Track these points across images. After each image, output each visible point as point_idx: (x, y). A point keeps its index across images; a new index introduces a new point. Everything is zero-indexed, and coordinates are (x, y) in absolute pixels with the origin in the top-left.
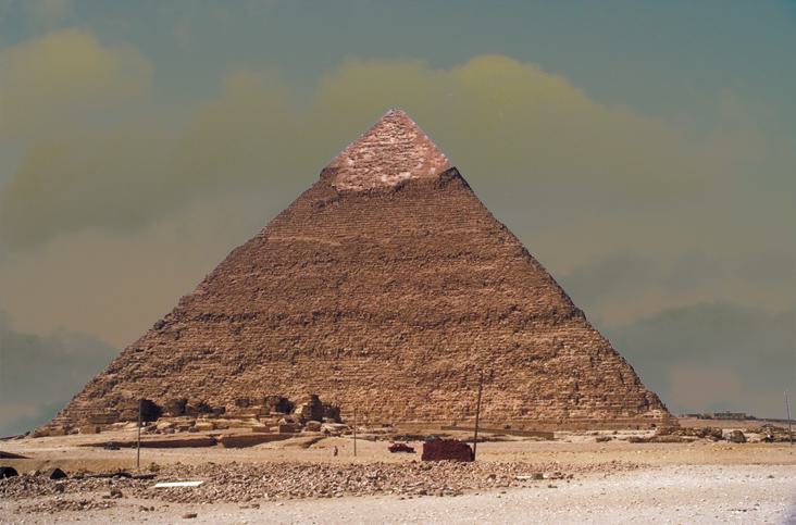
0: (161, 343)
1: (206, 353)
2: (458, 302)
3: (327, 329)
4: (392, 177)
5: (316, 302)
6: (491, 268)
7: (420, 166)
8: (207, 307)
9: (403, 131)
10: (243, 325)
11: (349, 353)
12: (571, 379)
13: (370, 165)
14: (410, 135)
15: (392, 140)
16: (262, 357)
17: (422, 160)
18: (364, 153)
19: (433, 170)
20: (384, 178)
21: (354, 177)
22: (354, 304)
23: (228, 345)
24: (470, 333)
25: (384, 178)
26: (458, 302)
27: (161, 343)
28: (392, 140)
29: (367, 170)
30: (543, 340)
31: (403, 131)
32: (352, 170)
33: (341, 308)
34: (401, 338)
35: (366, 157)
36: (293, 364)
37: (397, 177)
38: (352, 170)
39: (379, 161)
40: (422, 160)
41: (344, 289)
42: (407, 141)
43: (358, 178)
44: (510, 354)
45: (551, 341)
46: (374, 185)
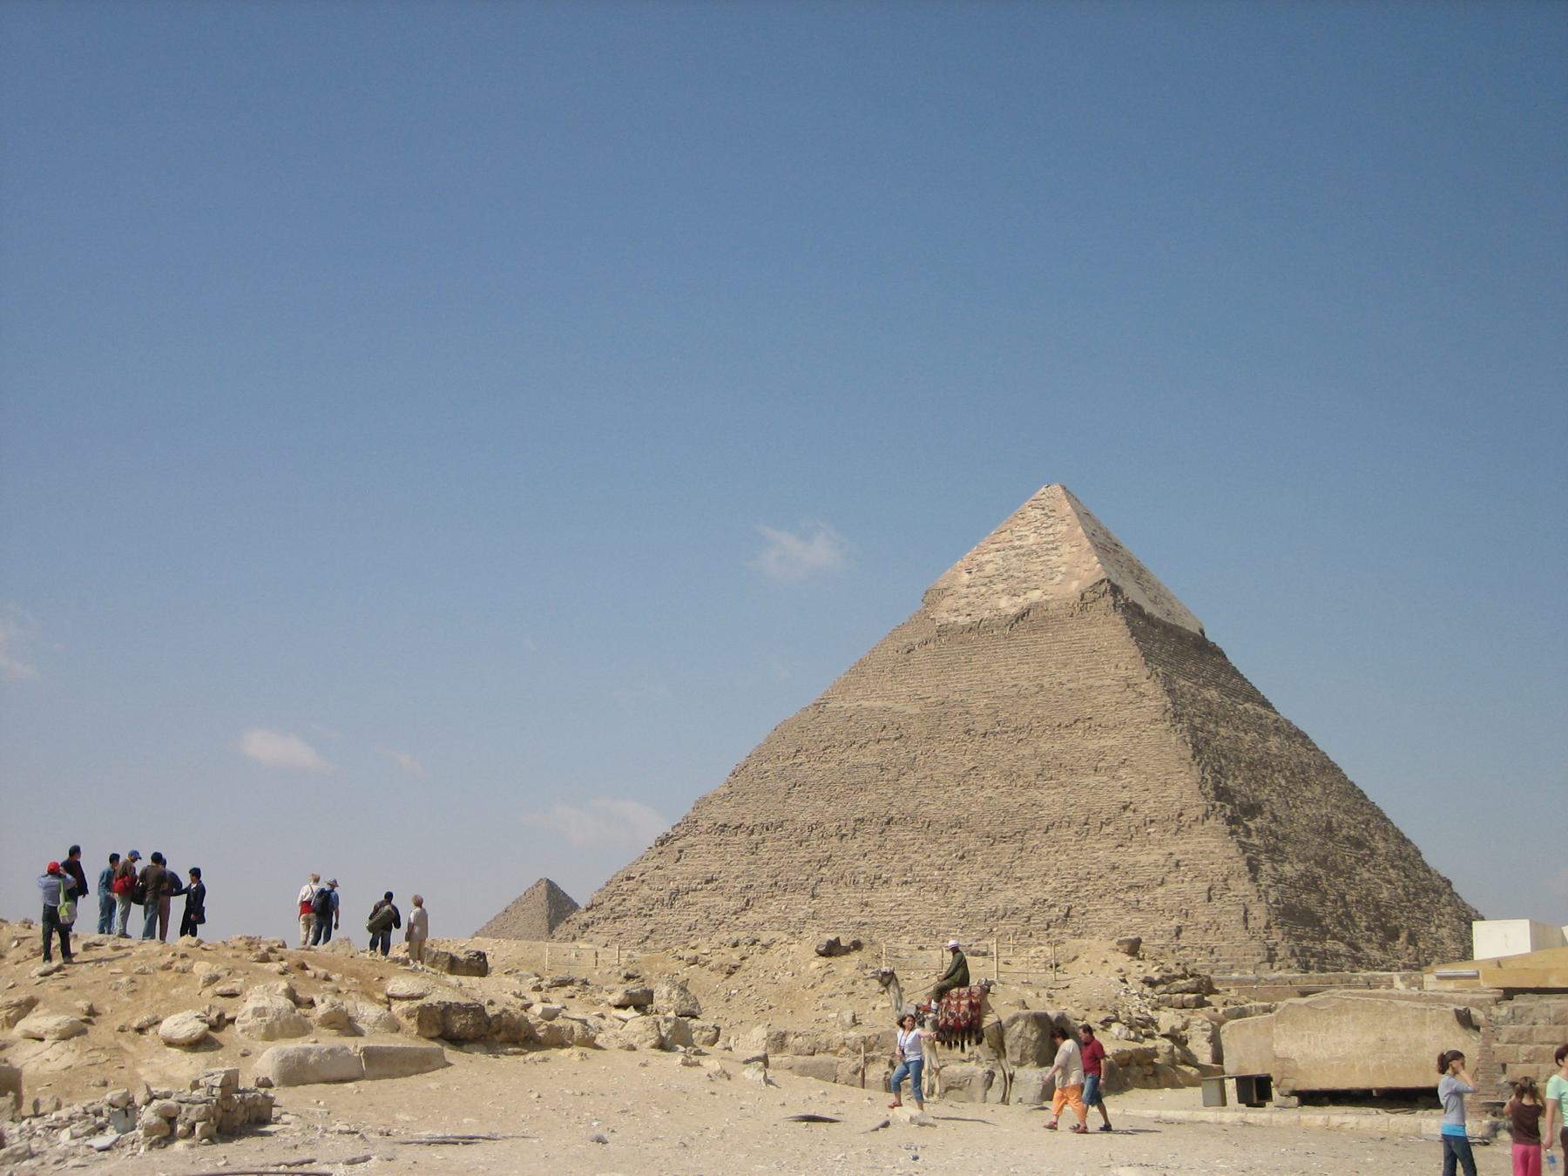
1: (707, 882)
2: (1051, 800)
3: (870, 845)
5: (866, 802)
7: (1059, 578)
8: (721, 814)
9: (1050, 521)
10: (764, 841)
13: (990, 580)
14: (1059, 528)
15: (1032, 539)
16: (778, 886)
19: (1075, 584)
21: (964, 601)
22: (911, 805)
23: (735, 870)
26: (1051, 800)
29: (984, 589)
31: (1050, 521)
33: (893, 812)
35: (989, 569)
36: (813, 896)
37: (1021, 600)
38: (964, 591)
39: (1005, 575)
41: (908, 781)
42: (1051, 538)
46: (986, 614)
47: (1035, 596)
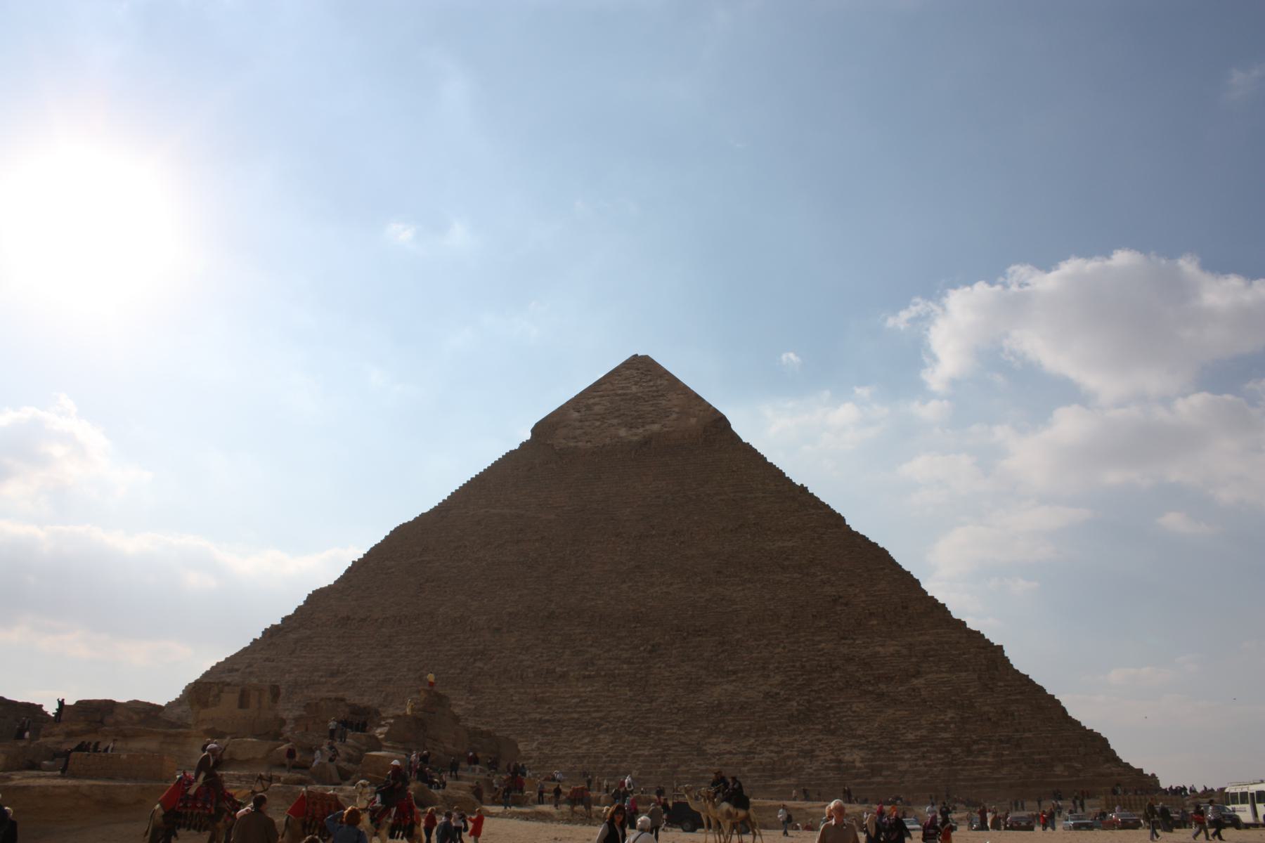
0: (267, 659)
1: (333, 675)
4: (634, 430)
6: (790, 544)
7: (674, 416)
11: (564, 676)
12: (950, 714)
14: (659, 382)
15: (634, 389)
17: (676, 409)
18: (595, 404)
19: (693, 421)
20: (623, 432)
21: (578, 432)
24: (765, 641)
25: (623, 432)
27: (267, 659)
28: (634, 389)
29: (598, 423)
30: (891, 649)
32: (577, 424)
34: (650, 652)
37: (641, 430)
40: (676, 409)
43: (585, 433)
44: (837, 674)
45: (905, 652)
46: (608, 441)
47: (656, 427)
